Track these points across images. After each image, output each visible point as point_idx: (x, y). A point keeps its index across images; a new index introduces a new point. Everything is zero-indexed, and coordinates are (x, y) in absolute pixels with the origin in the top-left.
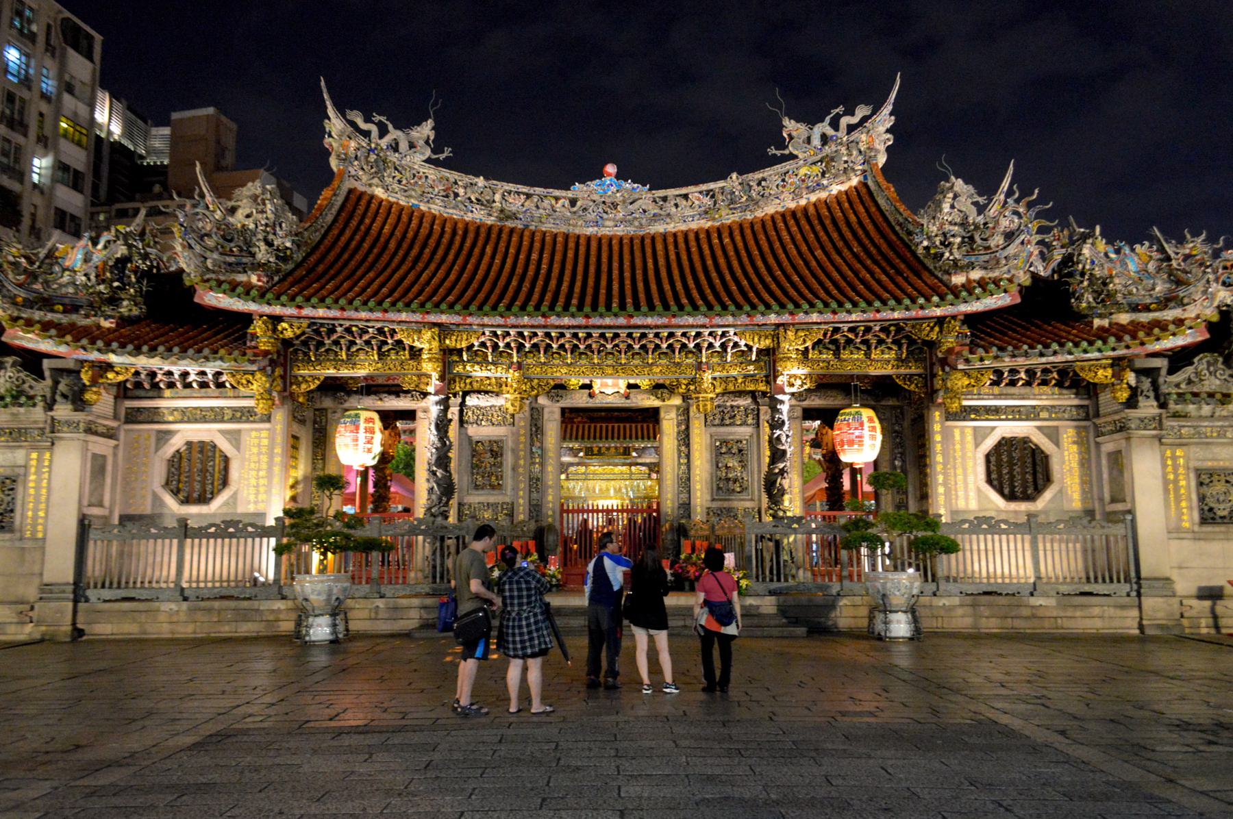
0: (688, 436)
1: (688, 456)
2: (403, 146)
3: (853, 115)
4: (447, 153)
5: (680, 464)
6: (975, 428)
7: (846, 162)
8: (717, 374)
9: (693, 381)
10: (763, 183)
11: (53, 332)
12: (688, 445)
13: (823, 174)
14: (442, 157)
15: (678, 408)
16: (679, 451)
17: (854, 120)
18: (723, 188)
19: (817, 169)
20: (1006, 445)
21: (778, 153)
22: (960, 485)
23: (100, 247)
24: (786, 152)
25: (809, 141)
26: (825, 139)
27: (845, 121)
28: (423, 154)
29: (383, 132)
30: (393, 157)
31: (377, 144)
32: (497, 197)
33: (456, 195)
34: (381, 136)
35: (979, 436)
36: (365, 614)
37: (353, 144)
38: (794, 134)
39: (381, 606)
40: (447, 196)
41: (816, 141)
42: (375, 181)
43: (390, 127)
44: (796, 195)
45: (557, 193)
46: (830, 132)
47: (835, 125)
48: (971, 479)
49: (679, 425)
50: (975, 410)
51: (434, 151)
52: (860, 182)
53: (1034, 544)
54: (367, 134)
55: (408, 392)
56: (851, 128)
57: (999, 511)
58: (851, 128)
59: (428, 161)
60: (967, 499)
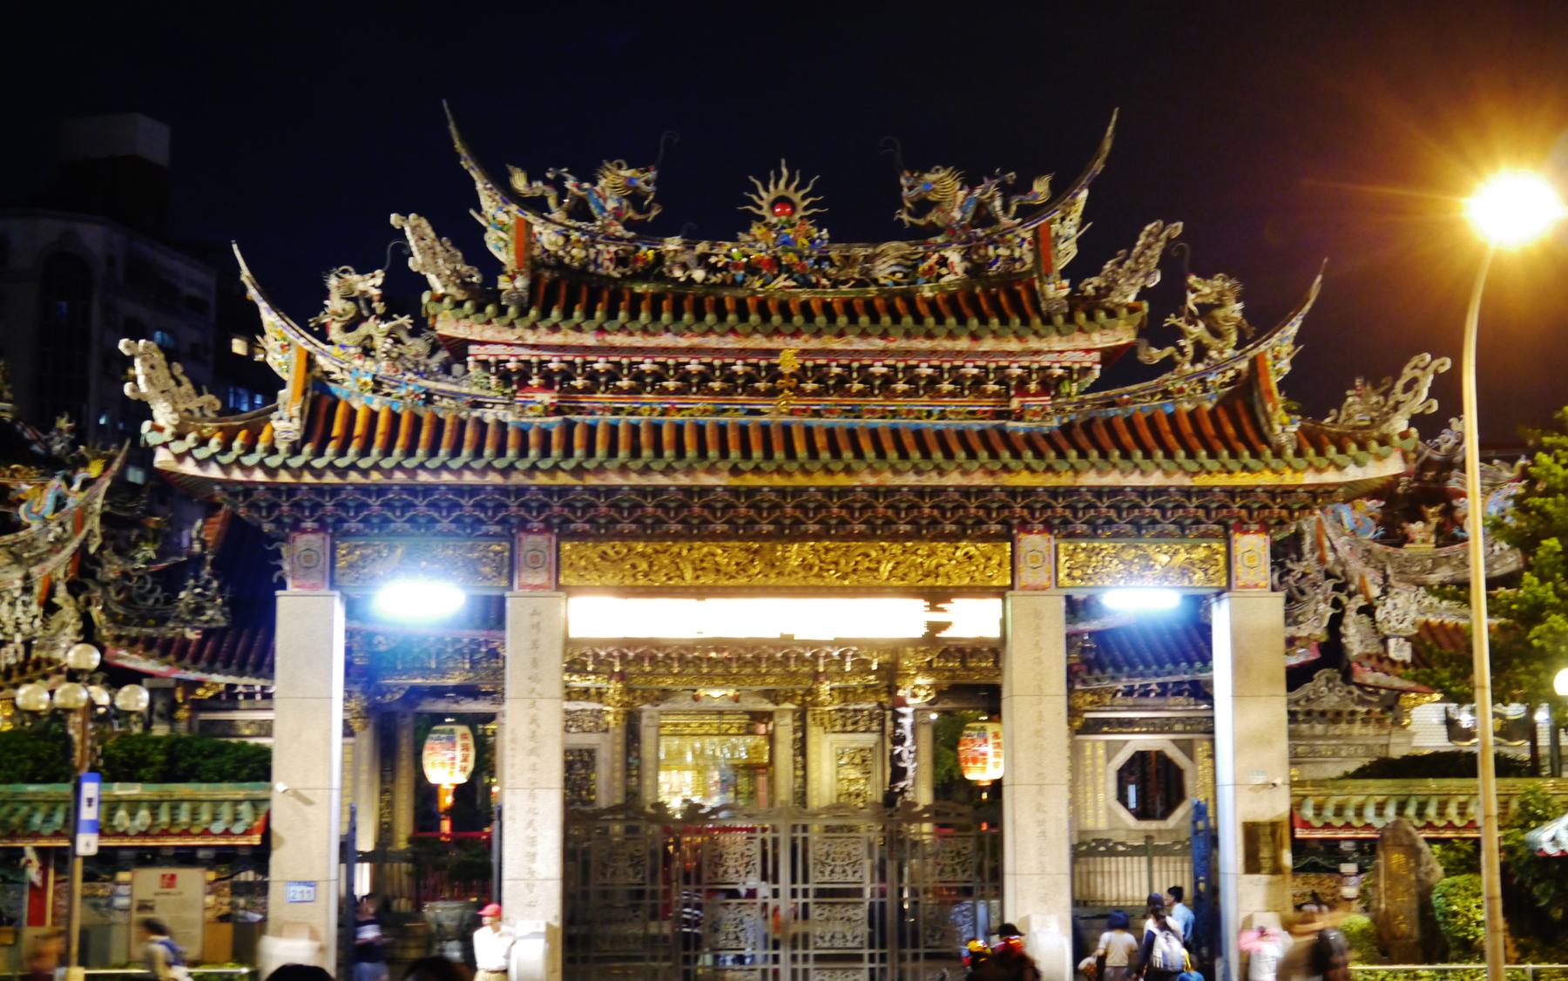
1: (804, 768)
5: (796, 777)
6: (1107, 742)
8: (836, 684)
9: (809, 692)
11: (140, 646)
15: (794, 712)
16: (795, 762)
20: (1140, 758)
22: (1090, 802)
23: (76, 487)
35: (1111, 749)
48: (1101, 796)
49: (795, 731)
50: (1107, 722)
53: (1150, 864)
55: (487, 694)
57: (1129, 831)
60: (1096, 816)
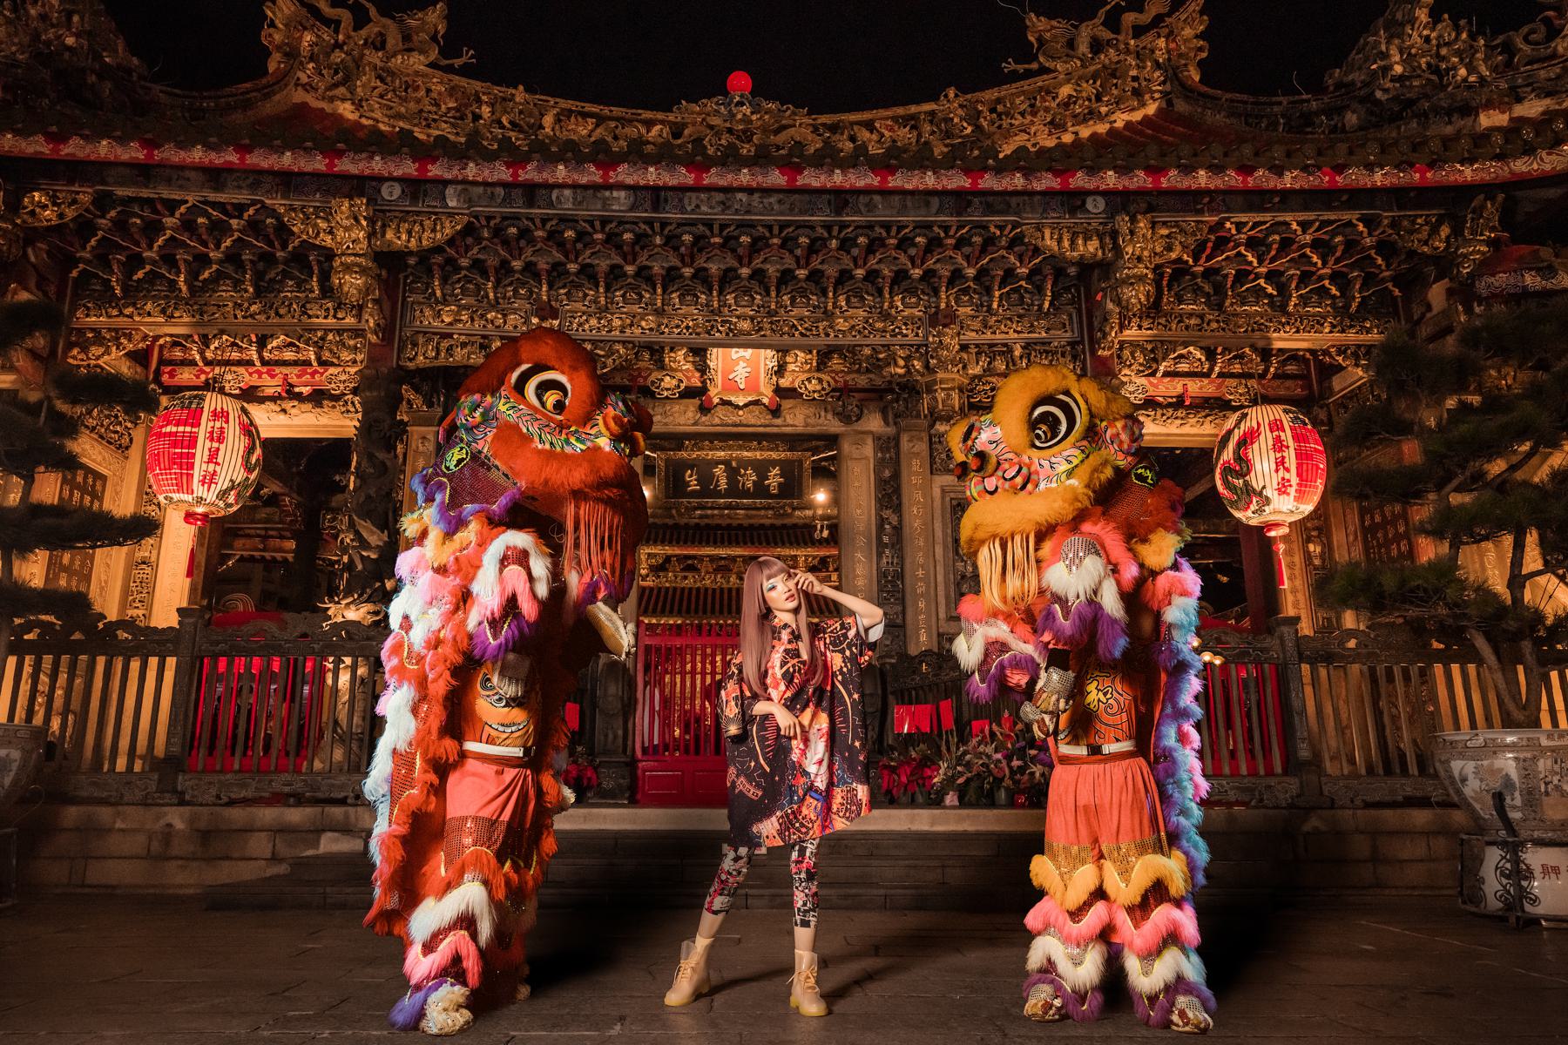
0: (897, 491)
2: (393, 40)
3: (1141, 11)
4: (467, 56)
7: (1135, 79)
10: (1000, 108)
12: (898, 509)
13: (1098, 99)
14: (457, 62)
15: (877, 438)
16: (881, 522)
17: (1145, 18)
18: (932, 113)
19: (1088, 89)
21: (1021, 68)
24: (1035, 66)
25: (1071, 44)
26: (1097, 46)
27: (1130, 18)
28: (421, 52)
29: (361, 20)
30: (375, 57)
31: (349, 37)
32: (548, 120)
33: (477, 117)
34: (358, 26)
36: (136, 844)
37: (308, 37)
38: (1048, 35)
39: (179, 825)
40: (462, 118)
41: (1083, 48)
42: (342, 90)
43: (373, 12)
44: (1056, 126)
45: (647, 115)
46: (1106, 35)
47: (1113, 23)
51: (444, 53)
52: (1159, 110)
54: (334, 24)
55: (336, 398)
56: (1139, 31)
58: (1139, 31)
59: (432, 65)
